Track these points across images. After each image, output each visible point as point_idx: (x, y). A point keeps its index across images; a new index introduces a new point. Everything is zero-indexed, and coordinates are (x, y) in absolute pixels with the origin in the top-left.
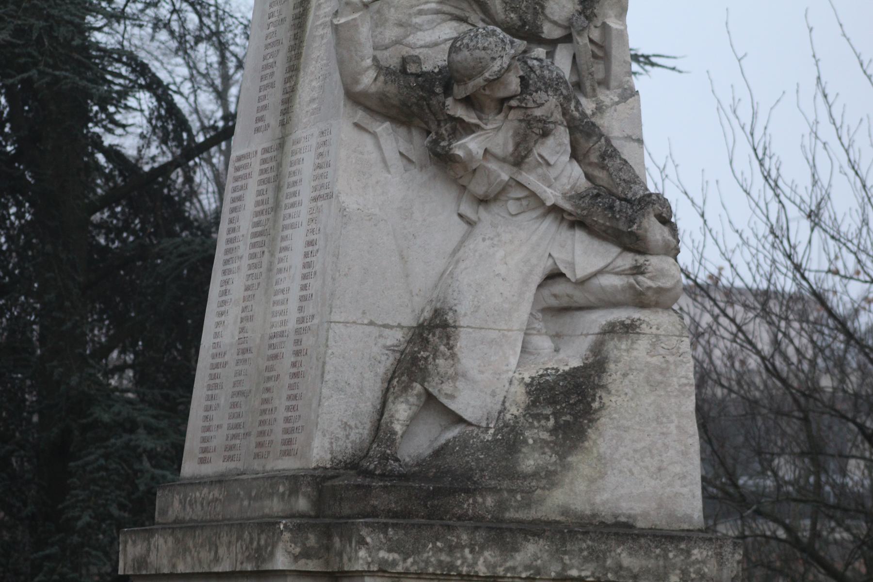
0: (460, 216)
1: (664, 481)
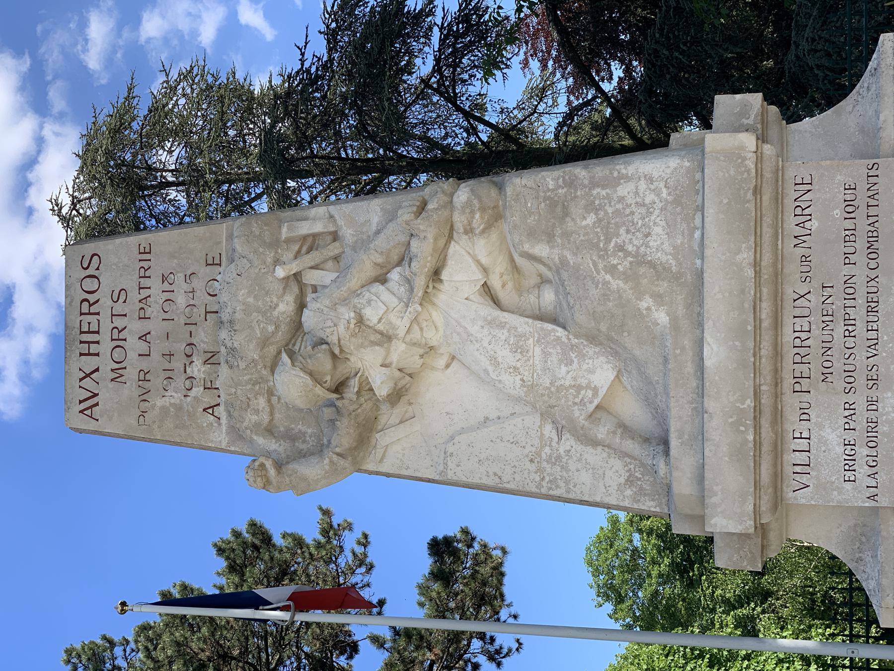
0: (448, 366)
1: (656, 199)
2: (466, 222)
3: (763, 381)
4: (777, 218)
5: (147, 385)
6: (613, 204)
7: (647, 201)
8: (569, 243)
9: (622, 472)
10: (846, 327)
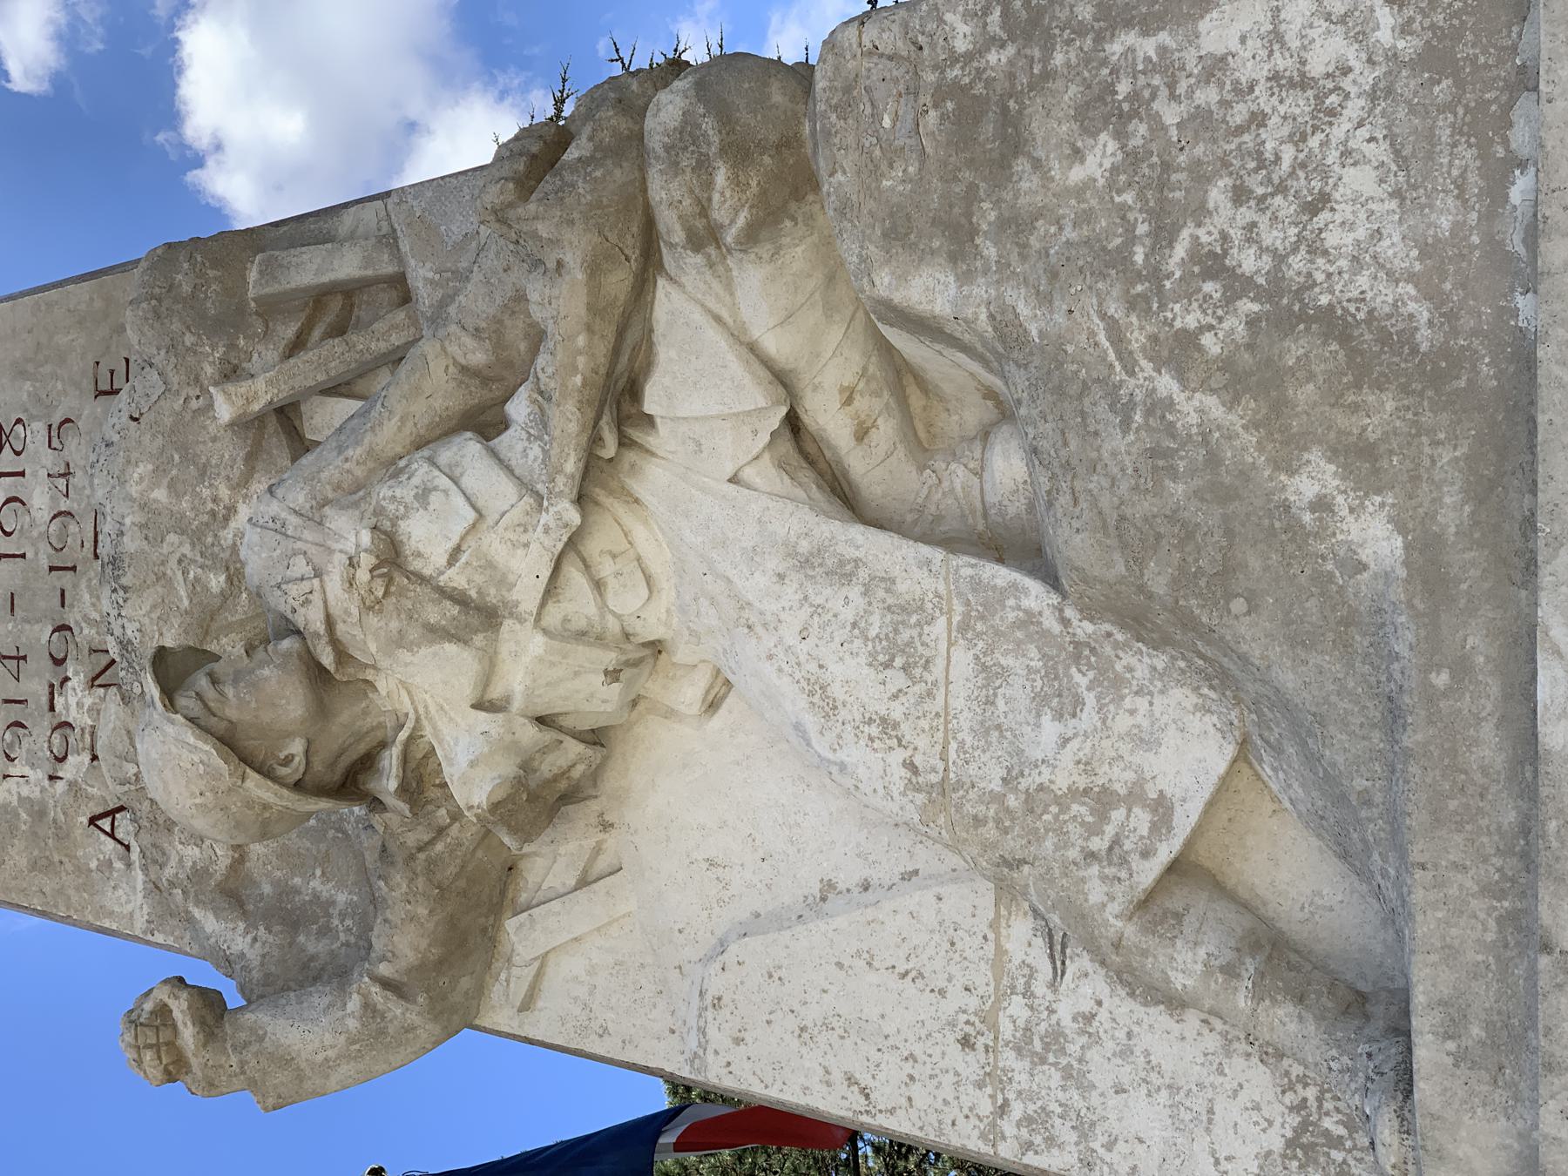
2: (687, 202)
6: (1181, 88)
7: (1316, 68)
8: (1023, 257)
9: (1276, 1111)
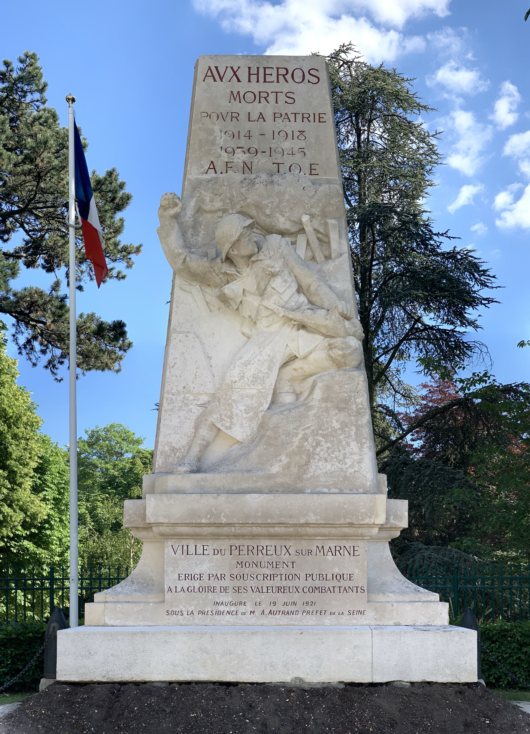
2: (337, 345)
3: (237, 528)
4: (334, 536)
5: (229, 119)
6: (346, 439)
7: (346, 460)
8: (322, 411)
10: (269, 575)
